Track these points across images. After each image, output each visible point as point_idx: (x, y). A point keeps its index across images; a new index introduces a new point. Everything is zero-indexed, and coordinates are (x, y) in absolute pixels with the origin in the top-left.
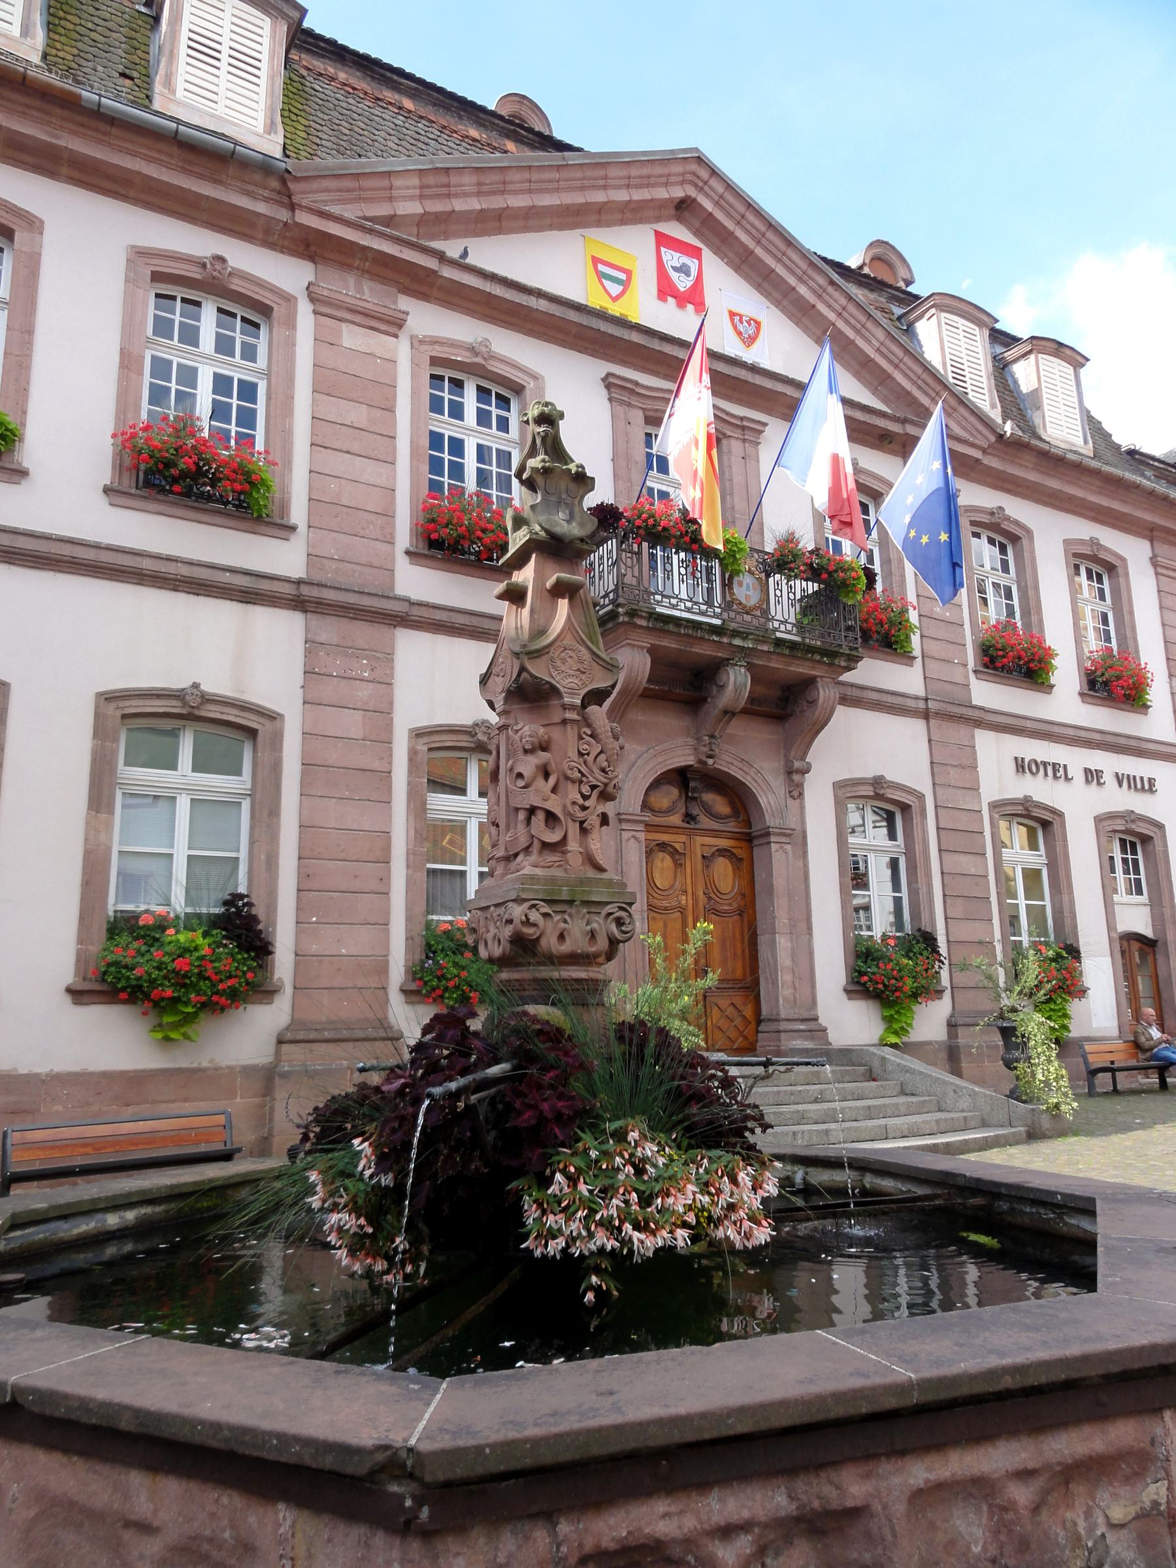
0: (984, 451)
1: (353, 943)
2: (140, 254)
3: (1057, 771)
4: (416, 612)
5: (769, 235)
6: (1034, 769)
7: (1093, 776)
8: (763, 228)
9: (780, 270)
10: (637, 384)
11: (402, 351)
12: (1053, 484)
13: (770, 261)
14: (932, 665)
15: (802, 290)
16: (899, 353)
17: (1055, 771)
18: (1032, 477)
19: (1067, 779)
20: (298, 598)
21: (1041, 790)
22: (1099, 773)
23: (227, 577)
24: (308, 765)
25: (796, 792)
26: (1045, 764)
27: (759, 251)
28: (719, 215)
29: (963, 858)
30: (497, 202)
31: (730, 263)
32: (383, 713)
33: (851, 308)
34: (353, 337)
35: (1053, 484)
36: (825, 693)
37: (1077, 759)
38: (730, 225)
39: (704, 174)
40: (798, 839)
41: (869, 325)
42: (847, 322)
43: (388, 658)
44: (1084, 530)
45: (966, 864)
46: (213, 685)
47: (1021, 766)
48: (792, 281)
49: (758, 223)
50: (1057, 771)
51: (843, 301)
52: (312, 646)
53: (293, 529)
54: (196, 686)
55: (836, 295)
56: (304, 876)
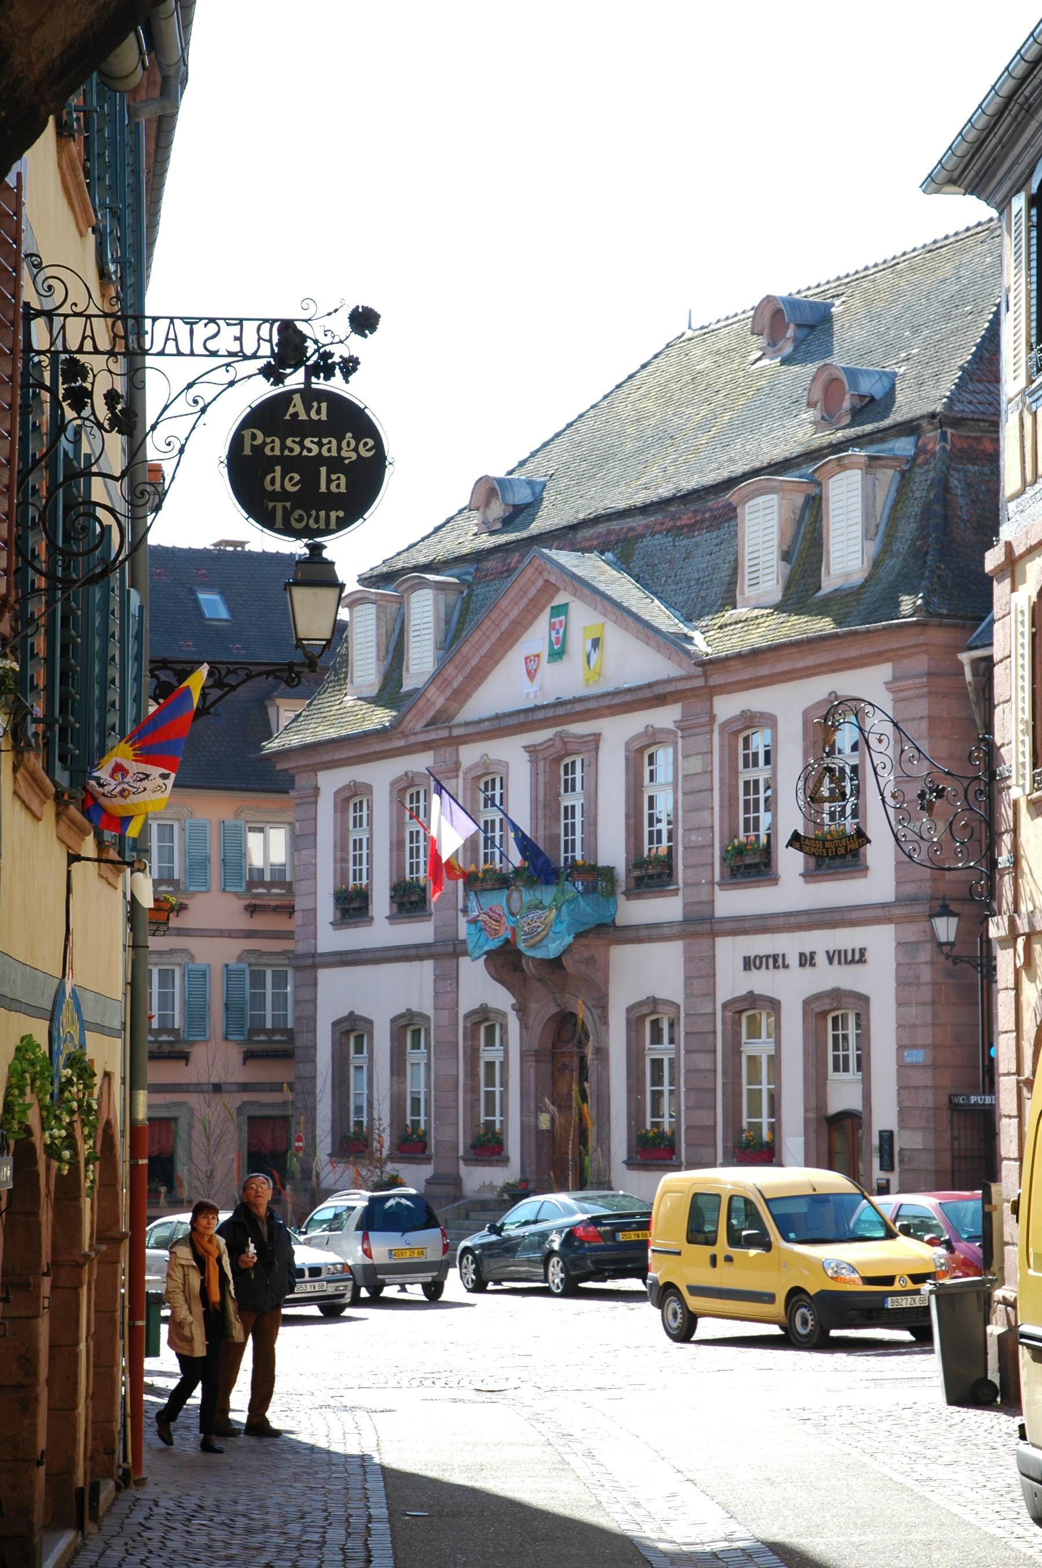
3: (777, 961)
6: (758, 964)
7: (807, 960)
12: (765, 670)
17: (775, 961)
21: (762, 982)
22: (812, 954)
26: (767, 957)
30: (468, 669)
37: (788, 944)
47: (749, 963)
50: (777, 961)
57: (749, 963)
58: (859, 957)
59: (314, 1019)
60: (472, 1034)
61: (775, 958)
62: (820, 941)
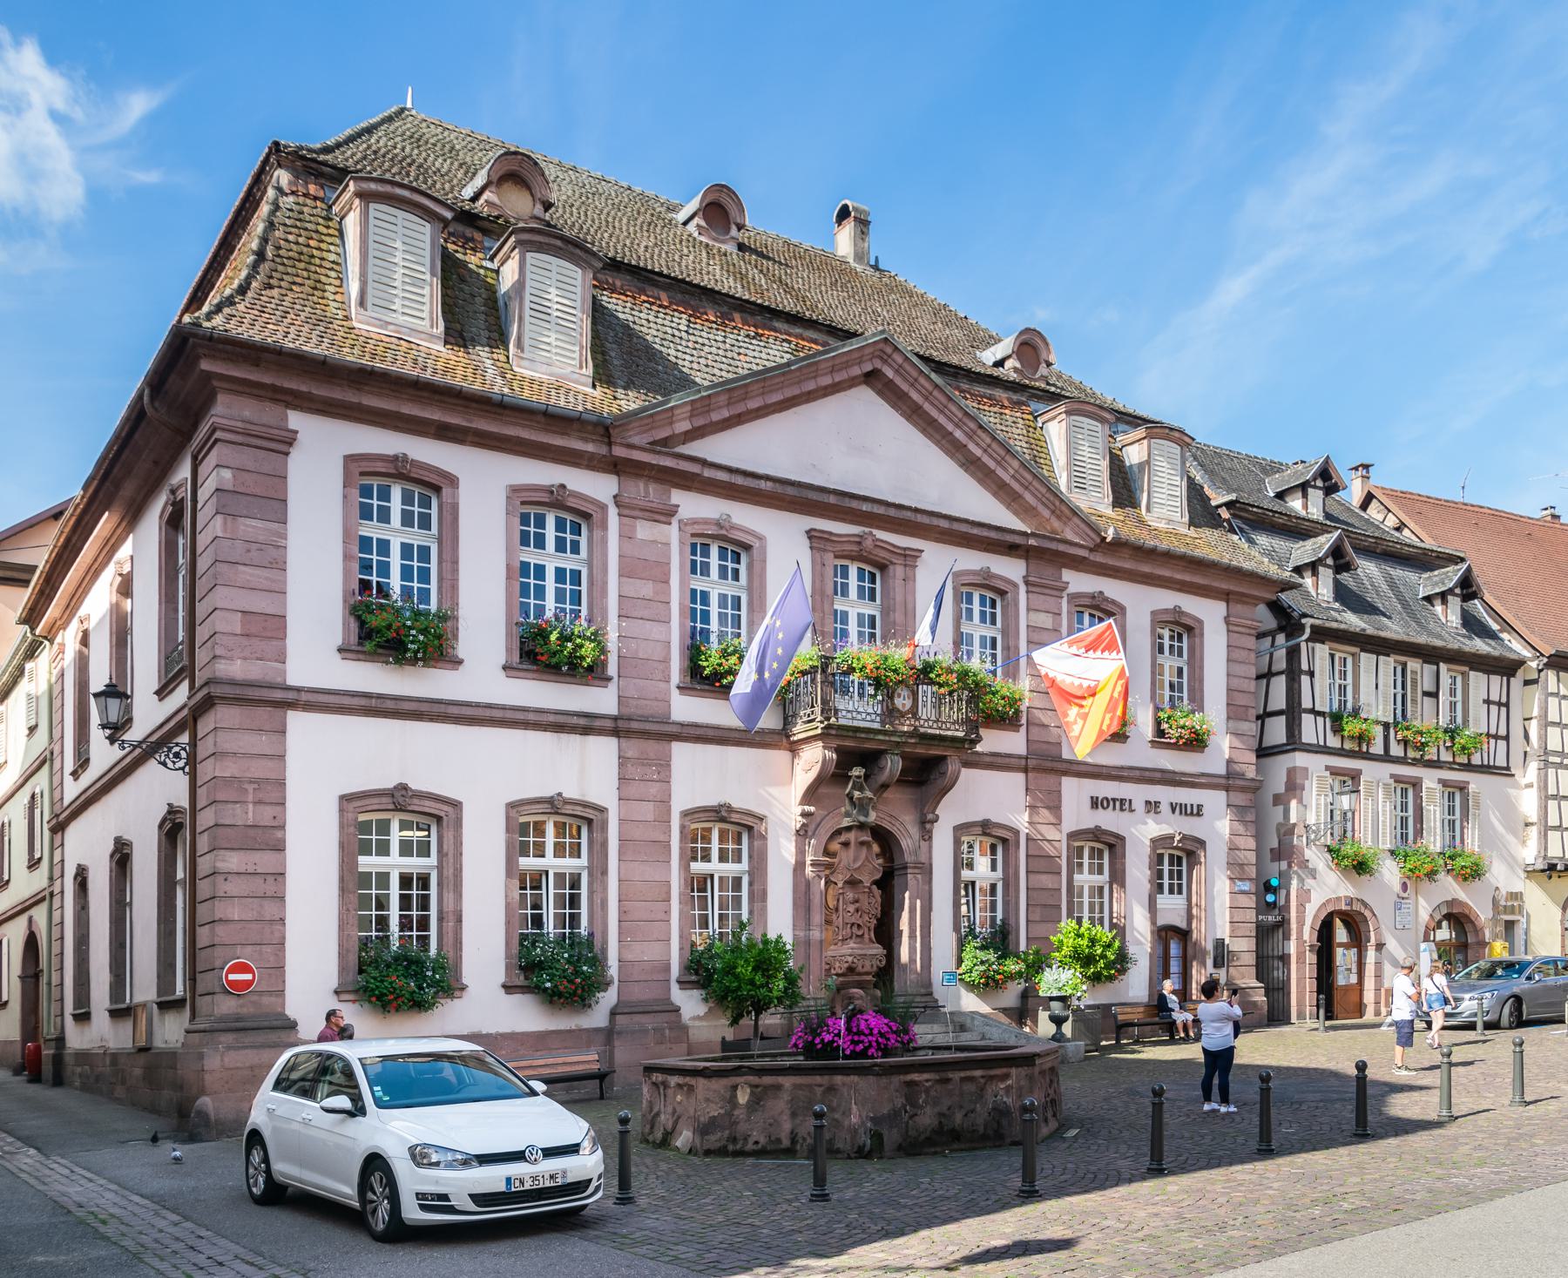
0: (1091, 550)
1: (646, 952)
2: (515, 490)
3: (1123, 804)
4: (685, 730)
5: (936, 393)
7: (1152, 807)
8: (930, 388)
9: (942, 420)
10: (831, 533)
11: (672, 533)
12: (1146, 568)
13: (934, 413)
14: (1034, 730)
15: (958, 434)
16: (1029, 477)
17: (1122, 804)
18: (1128, 565)
19: (1132, 811)
20: (617, 727)
21: (1108, 820)
22: (1157, 804)
23: (575, 720)
24: (622, 841)
25: (927, 836)
26: (1114, 800)
27: (927, 406)
28: (898, 381)
29: (1044, 877)
30: (740, 408)
31: (903, 414)
32: (665, 802)
33: (994, 445)
34: (645, 530)
35: (1146, 568)
36: (952, 765)
38: (904, 387)
39: (889, 350)
40: (927, 870)
41: (1008, 458)
42: (991, 456)
43: (665, 765)
44: (1167, 599)
45: (1046, 881)
46: (569, 793)
47: (1095, 803)
48: (950, 427)
49: (927, 385)
50: (1123, 804)
51: (988, 440)
52: (623, 760)
53: (609, 679)
54: (560, 794)
55: (983, 436)
56: (623, 912)
57: (1095, 803)
58: (1197, 811)
59: (281, 784)
60: (688, 836)
61: (1122, 801)
62: (1165, 795)
